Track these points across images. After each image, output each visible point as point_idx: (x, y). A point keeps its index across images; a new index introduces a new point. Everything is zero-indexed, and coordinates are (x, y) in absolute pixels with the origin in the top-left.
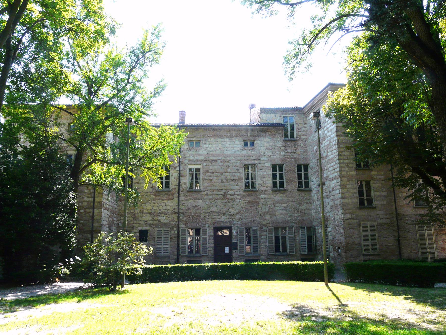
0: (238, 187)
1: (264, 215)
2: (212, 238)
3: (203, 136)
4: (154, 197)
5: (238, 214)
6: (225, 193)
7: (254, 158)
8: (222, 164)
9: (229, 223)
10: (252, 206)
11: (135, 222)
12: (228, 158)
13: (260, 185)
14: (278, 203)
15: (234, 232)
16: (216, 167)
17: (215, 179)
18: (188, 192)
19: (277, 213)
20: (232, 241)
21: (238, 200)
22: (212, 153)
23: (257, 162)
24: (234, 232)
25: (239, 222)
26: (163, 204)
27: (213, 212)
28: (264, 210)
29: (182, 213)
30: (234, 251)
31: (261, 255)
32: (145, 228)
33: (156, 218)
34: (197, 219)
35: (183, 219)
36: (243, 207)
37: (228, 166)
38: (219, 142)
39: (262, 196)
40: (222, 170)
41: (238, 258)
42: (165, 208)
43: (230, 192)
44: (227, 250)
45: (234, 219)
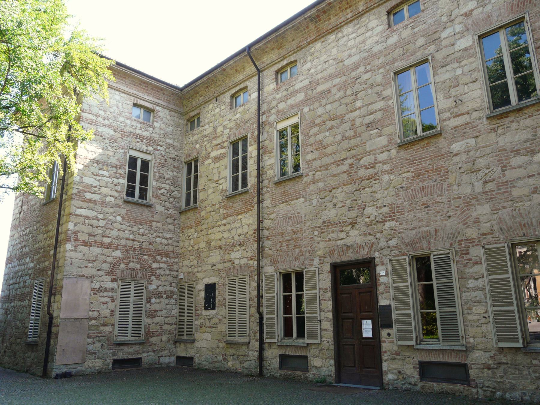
0: (383, 141)
1: (468, 205)
2: (329, 295)
3: (300, 48)
4: (225, 212)
5: (390, 216)
6: (351, 165)
7: (421, 42)
8: (341, 93)
9: (366, 249)
10: (426, 184)
11: (200, 269)
12: (354, 74)
13: (448, 115)
14: (517, 152)
15: (383, 273)
16: (329, 107)
17: (327, 137)
18: (278, 184)
19: (516, 193)
20: (376, 300)
21: (386, 178)
22: (319, 76)
23: (432, 48)
24: (383, 273)
25: (393, 243)
26: (237, 224)
27: (327, 223)
28: (468, 190)
29: (268, 239)
30: (384, 333)
31: (474, 348)
32: (211, 281)
33: (227, 257)
34: (296, 247)
35: (270, 252)
36: (402, 193)
37: (356, 94)
38: (333, 44)
39: (456, 147)
40: (342, 110)
41: (398, 354)
42: (239, 231)
43: (365, 161)
44: (367, 328)
45: (378, 235)
